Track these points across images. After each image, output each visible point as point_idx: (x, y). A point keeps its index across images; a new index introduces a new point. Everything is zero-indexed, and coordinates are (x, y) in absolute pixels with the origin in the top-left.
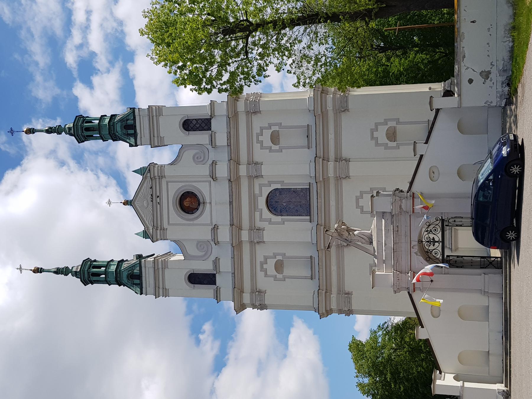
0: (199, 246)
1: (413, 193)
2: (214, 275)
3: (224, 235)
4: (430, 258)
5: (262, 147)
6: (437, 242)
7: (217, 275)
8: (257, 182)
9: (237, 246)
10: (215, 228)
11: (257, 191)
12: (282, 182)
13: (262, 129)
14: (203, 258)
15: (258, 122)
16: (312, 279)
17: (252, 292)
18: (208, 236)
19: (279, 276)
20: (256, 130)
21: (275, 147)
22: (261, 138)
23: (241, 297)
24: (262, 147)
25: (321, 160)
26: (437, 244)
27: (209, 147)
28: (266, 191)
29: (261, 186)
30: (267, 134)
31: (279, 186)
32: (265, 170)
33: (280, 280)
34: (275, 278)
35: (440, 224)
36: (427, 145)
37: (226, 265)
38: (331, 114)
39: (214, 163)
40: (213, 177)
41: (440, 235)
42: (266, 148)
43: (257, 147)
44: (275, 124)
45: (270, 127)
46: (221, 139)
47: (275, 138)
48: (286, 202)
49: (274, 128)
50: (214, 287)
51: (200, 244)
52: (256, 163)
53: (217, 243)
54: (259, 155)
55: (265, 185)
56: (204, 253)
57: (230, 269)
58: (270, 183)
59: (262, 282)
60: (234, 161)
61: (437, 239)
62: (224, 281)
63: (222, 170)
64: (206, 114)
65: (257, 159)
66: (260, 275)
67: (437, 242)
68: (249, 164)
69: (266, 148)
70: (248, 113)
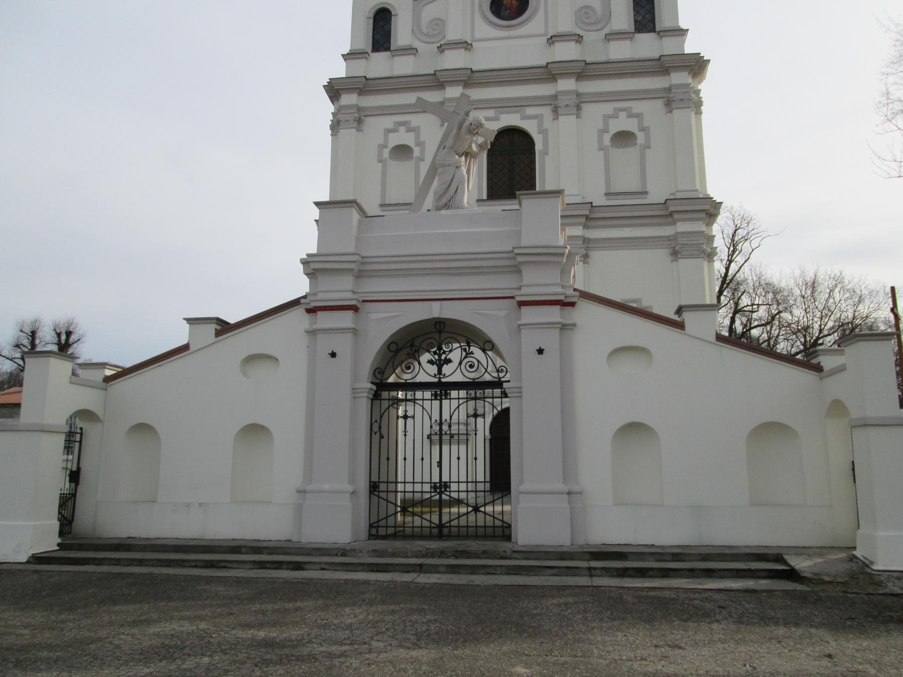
0: (438, 22)
1: (573, 304)
2: (388, 49)
3: (454, 60)
4: (397, 352)
5: (607, 118)
6: (440, 371)
7: (388, 53)
8: (546, 111)
9: (437, 81)
10: (466, 46)
11: (530, 111)
12: (545, 152)
13: (638, 116)
14: (416, 30)
15: (652, 109)
16: (382, 205)
17: (360, 109)
18: (453, 34)
19: (386, 153)
20: (637, 107)
21: (607, 138)
22: (623, 115)
23: (349, 90)
24: (607, 118)
25: (587, 212)
26: (433, 369)
27: (606, 30)
28: (530, 127)
29: (539, 118)
30: (630, 125)
31: (538, 147)
32: (567, 121)
33: (380, 154)
34: (384, 146)
35: (487, 378)
36: (713, 338)
37: (403, 66)
38: (667, 231)
39: (579, 39)
40: (552, 40)
41: (458, 377)
42: (606, 123)
43: (608, 108)
44: (648, 138)
45: (642, 129)
46: (620, 51)
47: (623, 138)
48: (512, 164)
49: (641, 138)
50: (369, 49)
51: (439, 23)
52: (579, 108)
53: (441, 49)
54: (594, 113)
55: (540, 124)
56: (425, 30)
57: (397, 72)
58: (543, 131)
59: (376, 126)
60: (584, 71)
61: (446, 369)
62: (380, 65)
63: (566, 52)
64: (663, 21)
65: (587, 108)
66: (388, 122)
67: (440, 371)
68: (578, 95)
69: (606, 123)
70: (669, 89)
